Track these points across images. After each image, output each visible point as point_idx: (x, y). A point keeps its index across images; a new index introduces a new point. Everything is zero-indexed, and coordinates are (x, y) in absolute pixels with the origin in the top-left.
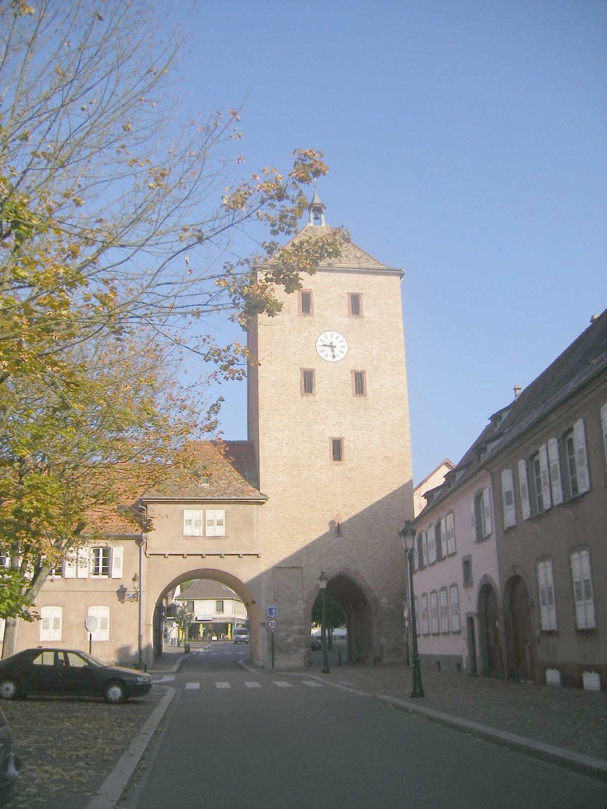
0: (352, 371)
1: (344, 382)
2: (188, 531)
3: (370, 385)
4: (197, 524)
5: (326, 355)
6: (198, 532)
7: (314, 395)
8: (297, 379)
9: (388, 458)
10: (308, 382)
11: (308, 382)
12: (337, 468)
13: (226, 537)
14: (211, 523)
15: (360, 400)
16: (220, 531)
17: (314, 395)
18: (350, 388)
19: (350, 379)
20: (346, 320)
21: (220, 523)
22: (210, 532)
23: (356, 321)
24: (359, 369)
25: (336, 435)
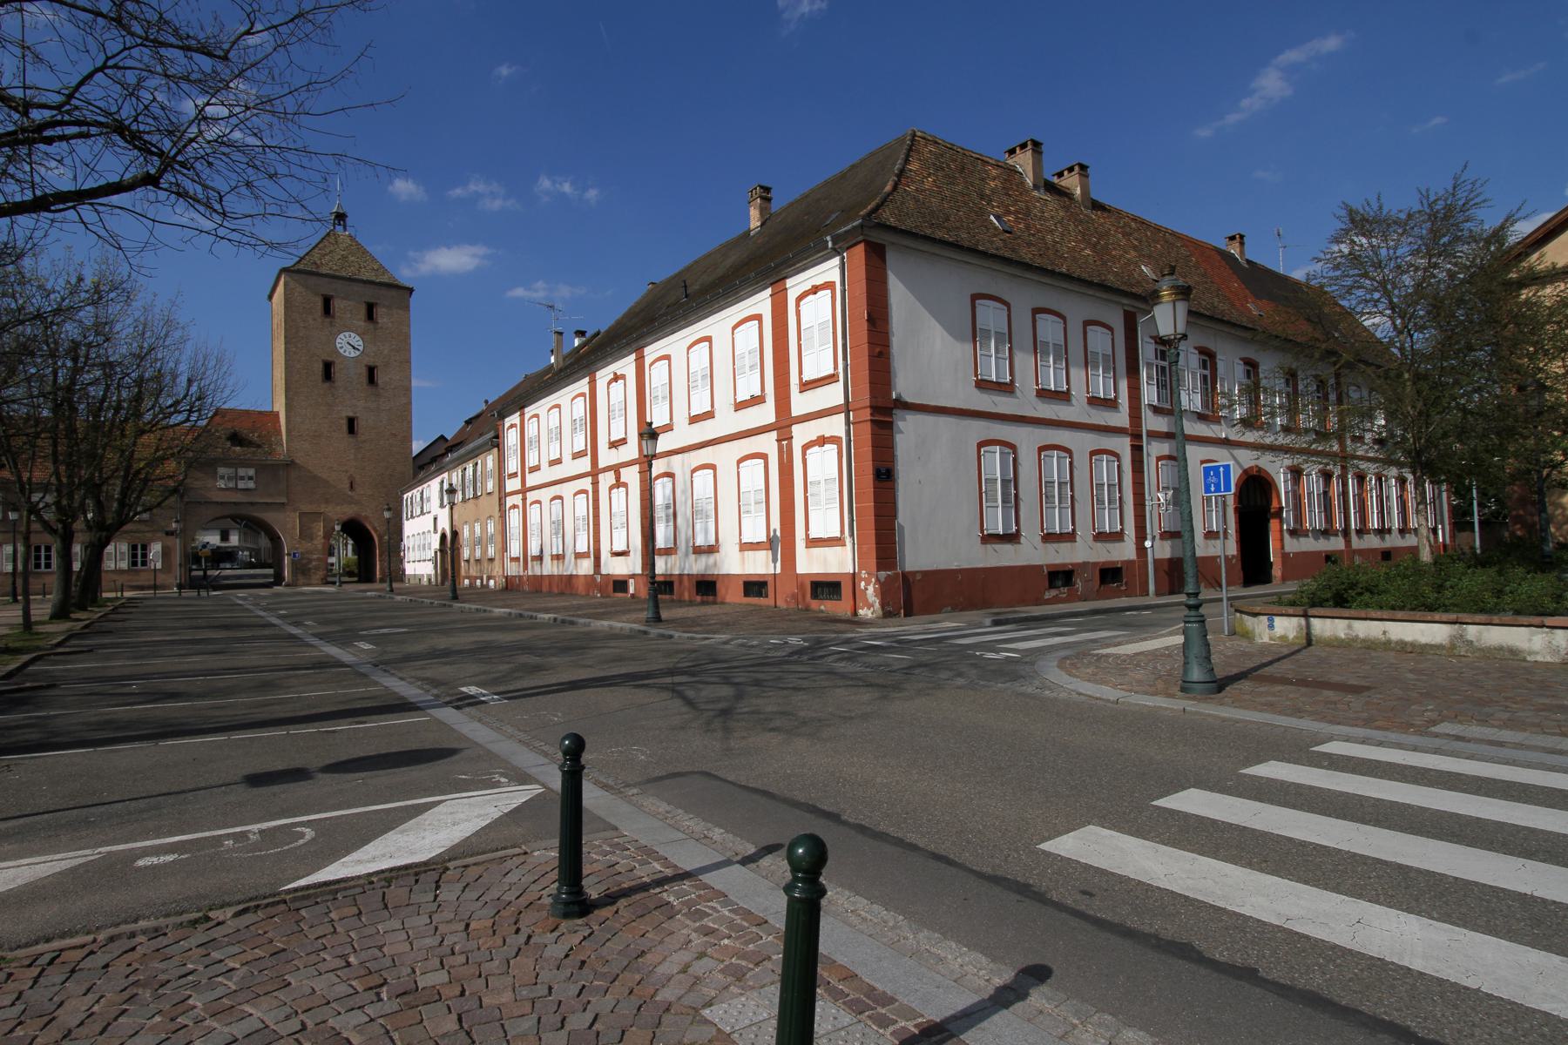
2: (221, 484)
3: (381, 378)
4: (230, 479)
6: (231, 485)
8: (319, 368)
10: (328, 369)
11: (328, 369)
14: (242, 478)
16: (251, 485)
18: (364, 380)
19: (364, 372)
21: (250, 478)
22: (241, 485)
23: (371, 326)
25: (351, 414)
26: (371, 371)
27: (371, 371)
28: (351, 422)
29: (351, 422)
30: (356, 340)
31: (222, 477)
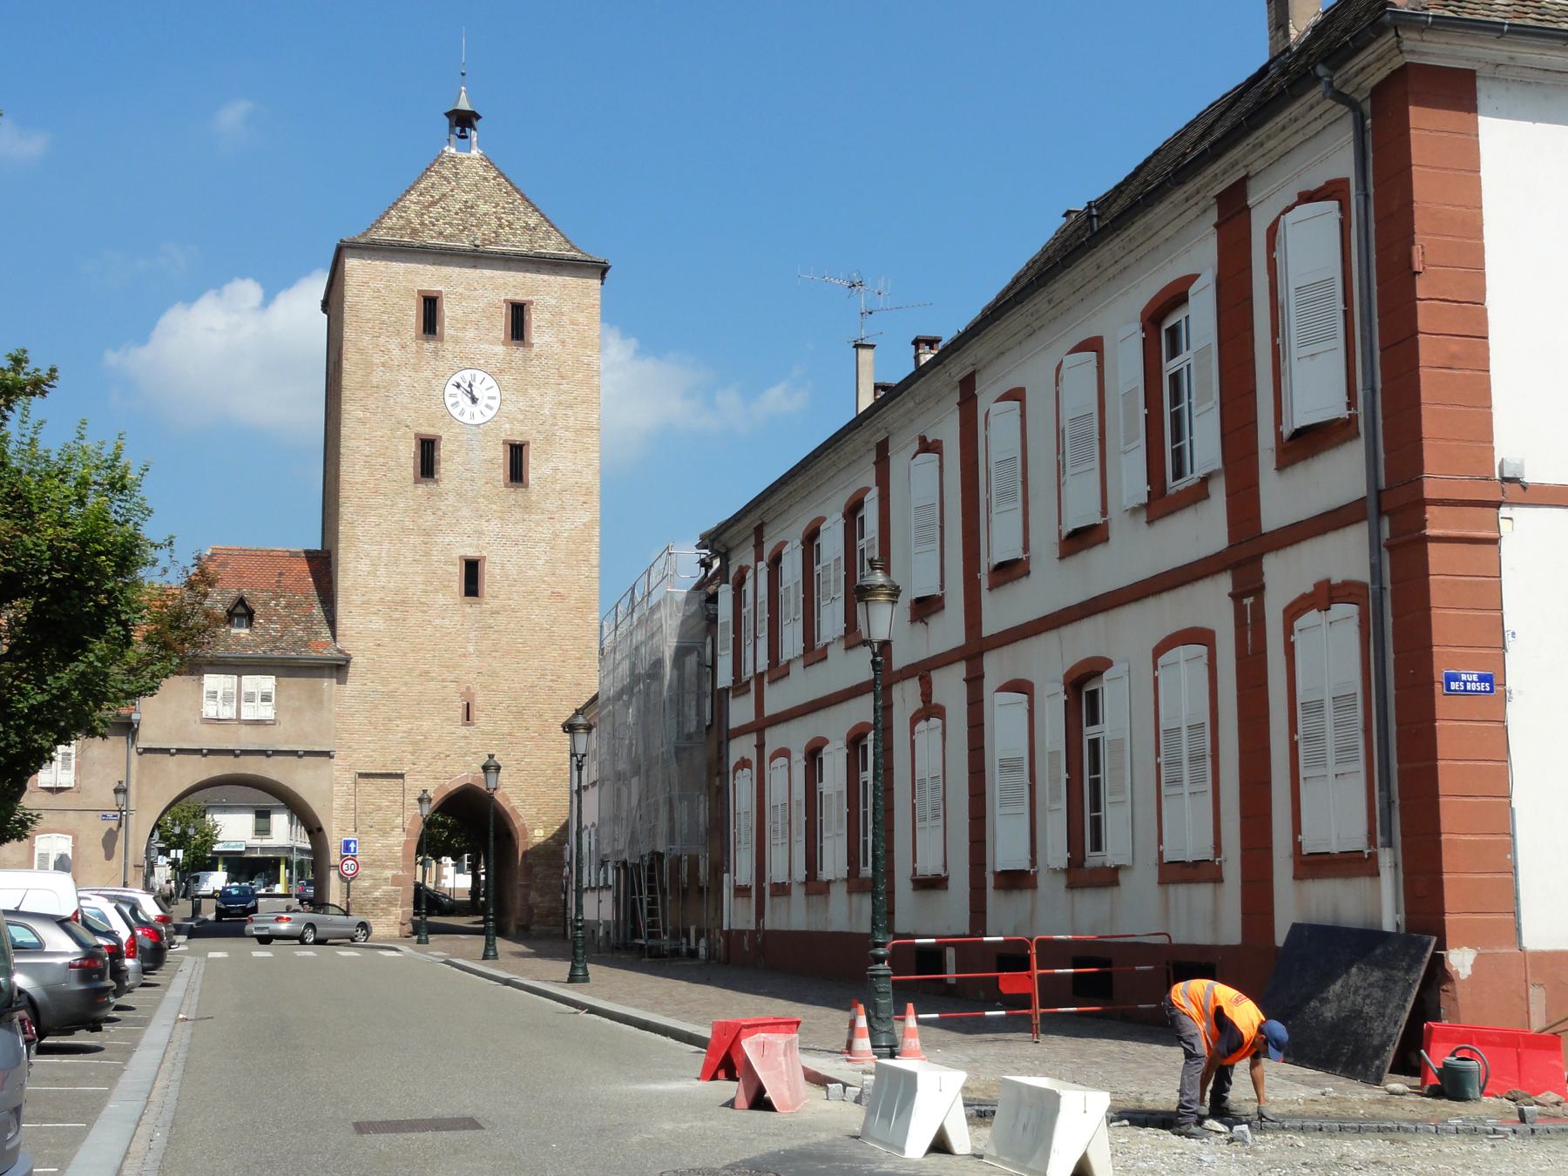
0: (505, 442)
1: (491, 461)
2: (210, 709)
3: (535, 468)
4: (227, 699)
5: (462, 413)
6: (228, 712)
7: (437, 481)
8: (408, 453)
9: (559, 595)
11: (427, 456)
12: (470, 608)
13: (274, 723)
14: (250, 698)
15: (515, 495)
16: (266, 711)
17: (437, 481)
18: (501, 472)
20: (500, 349)
21: (266, 698)
22: (248, 712)
24: (518, 439)
25: (472, 553)
26: (517, 454)
27: (517, 454)
28: (472, 569)
29: (472, 569)
30: (486, 387)
31: (213, 695)
